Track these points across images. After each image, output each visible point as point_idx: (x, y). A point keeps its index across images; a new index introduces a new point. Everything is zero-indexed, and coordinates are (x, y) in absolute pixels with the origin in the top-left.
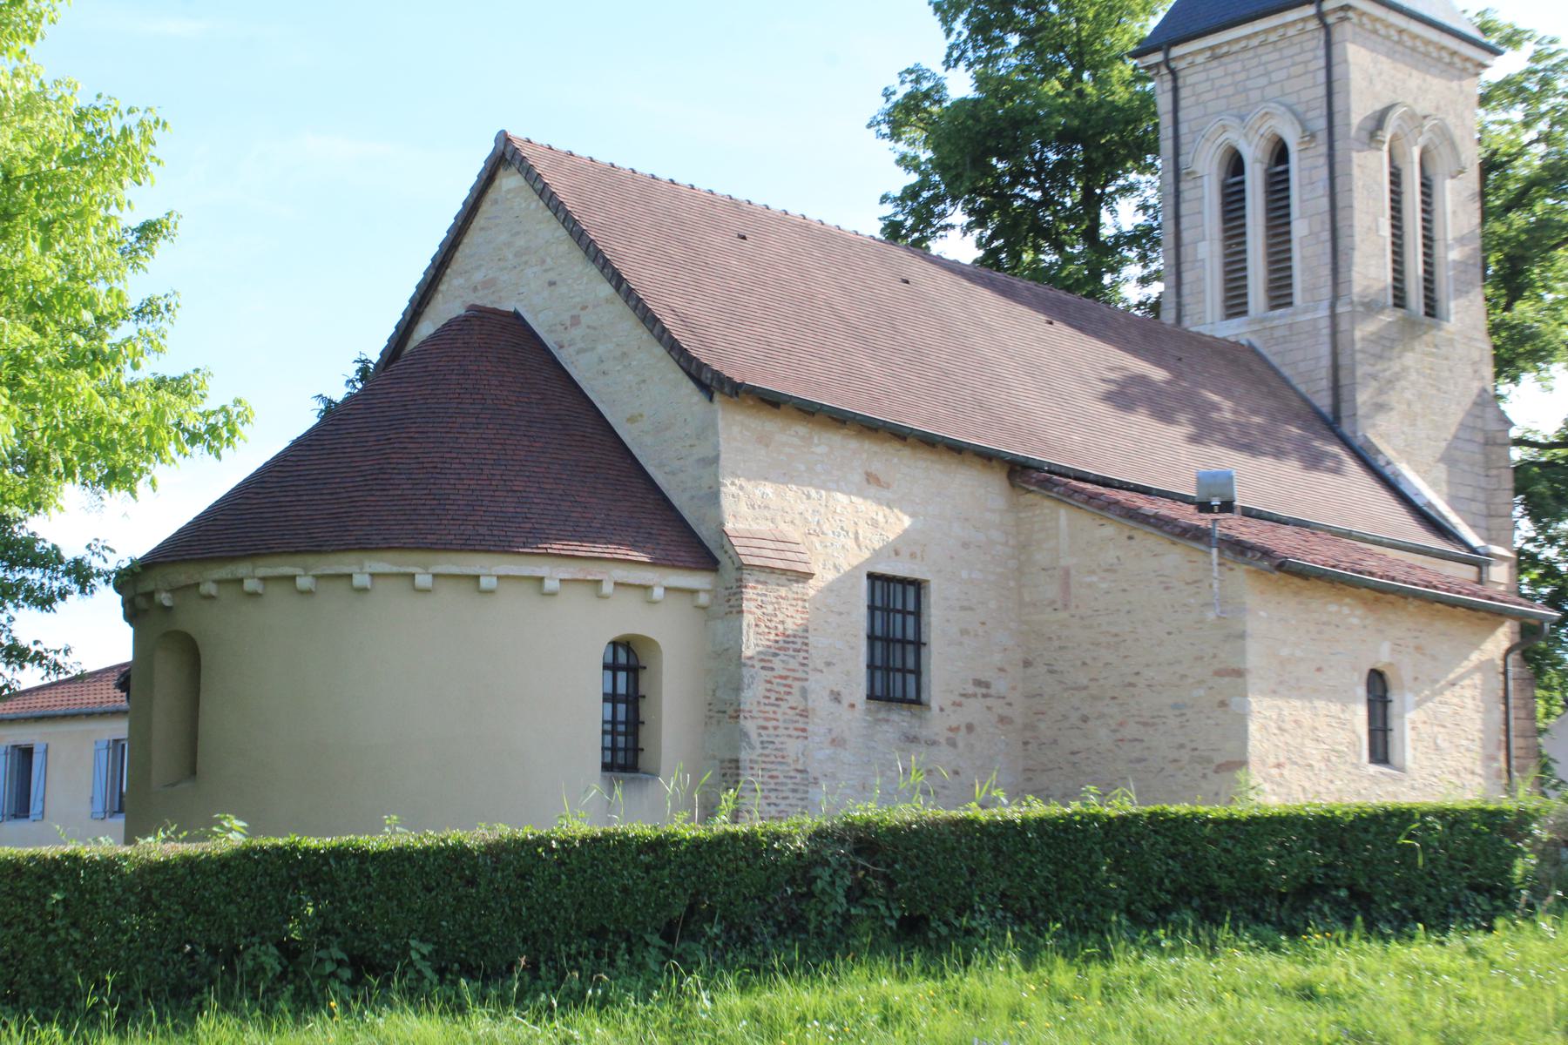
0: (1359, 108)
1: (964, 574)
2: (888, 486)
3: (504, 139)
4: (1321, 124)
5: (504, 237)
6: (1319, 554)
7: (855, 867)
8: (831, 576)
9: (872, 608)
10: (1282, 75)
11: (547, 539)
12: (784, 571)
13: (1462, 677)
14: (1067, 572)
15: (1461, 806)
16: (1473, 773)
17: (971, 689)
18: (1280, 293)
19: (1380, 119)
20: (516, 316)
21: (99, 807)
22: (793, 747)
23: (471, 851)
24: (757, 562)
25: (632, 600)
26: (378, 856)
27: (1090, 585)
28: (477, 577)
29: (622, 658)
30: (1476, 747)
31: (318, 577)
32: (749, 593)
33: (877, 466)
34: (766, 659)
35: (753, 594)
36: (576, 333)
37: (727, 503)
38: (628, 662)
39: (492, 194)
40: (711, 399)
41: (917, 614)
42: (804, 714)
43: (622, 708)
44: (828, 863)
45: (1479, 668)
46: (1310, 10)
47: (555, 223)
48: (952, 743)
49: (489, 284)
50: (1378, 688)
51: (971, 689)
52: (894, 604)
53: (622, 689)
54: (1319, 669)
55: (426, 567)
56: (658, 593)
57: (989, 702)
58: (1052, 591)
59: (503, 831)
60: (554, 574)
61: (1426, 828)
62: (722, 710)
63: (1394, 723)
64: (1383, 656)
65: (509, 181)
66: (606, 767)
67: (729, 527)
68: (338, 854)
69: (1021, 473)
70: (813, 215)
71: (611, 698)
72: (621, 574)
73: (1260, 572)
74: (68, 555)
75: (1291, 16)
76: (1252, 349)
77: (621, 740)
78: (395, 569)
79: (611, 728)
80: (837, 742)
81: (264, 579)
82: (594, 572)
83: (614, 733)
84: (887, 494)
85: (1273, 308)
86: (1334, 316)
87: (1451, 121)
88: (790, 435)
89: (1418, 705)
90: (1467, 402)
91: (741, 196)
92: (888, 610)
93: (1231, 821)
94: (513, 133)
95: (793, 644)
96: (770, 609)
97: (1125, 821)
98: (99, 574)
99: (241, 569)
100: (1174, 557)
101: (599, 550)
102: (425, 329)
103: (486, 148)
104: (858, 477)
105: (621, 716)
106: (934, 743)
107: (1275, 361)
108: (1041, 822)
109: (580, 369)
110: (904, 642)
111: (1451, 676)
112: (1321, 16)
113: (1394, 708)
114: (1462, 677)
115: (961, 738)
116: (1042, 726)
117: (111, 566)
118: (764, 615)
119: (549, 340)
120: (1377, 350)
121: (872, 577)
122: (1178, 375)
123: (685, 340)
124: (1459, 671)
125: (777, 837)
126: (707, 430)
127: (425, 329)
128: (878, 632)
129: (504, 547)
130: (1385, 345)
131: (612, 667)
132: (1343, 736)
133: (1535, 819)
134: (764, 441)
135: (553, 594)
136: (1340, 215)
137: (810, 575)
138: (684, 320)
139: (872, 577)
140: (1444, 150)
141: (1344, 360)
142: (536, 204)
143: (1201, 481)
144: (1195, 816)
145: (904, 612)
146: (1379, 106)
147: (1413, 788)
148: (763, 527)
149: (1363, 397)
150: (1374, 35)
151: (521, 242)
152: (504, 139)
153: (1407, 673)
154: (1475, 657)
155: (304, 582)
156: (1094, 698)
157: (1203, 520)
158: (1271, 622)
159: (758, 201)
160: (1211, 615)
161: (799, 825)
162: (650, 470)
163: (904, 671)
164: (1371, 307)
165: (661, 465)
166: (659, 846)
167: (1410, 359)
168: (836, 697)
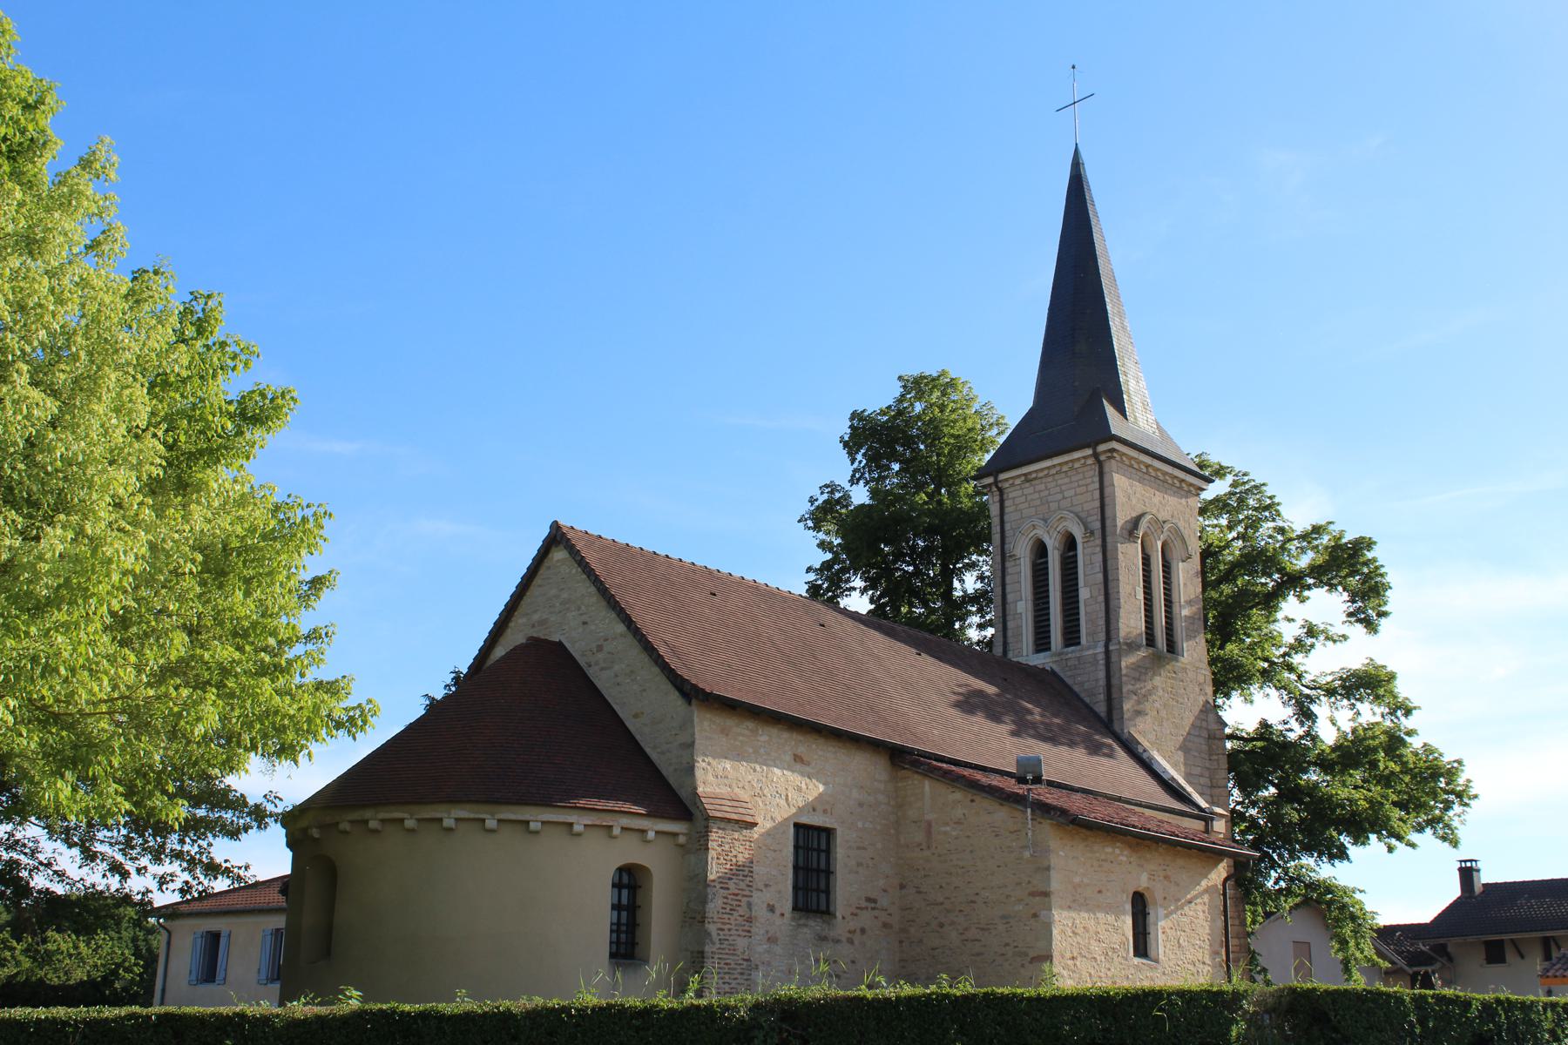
0: (1122, 516)
1: (860, 825)
2: (808, 764)
3: (555, 527)
4: (1098, 525)
5: (554, 592)
6: (1099, 813)
7: (781, 1029)
8: (769, 825)
9: (796, 847)
10: (1072, 492)
11: (576, 797)
12: (737, 822)
13: (1196, 897)
14: (929, 824)
15: (1194, 988)
17: (864, 904)
18: (1072, 635)
19: (1136, 522)
20: (560, 643)
21: (263, 976)
22: (741, 943)
23: (515, 1015)
24: (719, 814)
25: (633, 839)
26: (453, 1018)
27: (945, 833)
28: (527, 823)
29: (625, 879)
31: (419, 820)
32: (713, 836)
33: (801, 750)
34: (724, 881)
35: (715, 836)
36: (600, 655)
37: (699, 774)
38: (630, 881)
39: (546, 563)
40: (690, 703)
41: (828, 851)
42: (749, 920)
43: (624, 914)
44: (762, 1027)
46: (1089, 452)
47: (588, 583)
48: (850, 941)
49: (542, 622)
50: (1140, 907)
51: (864, 904)
52: (812, 844)
53: (624, 901)
55: (493, 814)
56: (651, 835)
57: (876, 913)
58: (919, 837)
59: (539, 1001)
60: (580, 821)
61: (1170, 1003)
62: (693, 915)
63: (1151, 929)
64: (1143, 882)
65: (559, 555)
66: (612, 955)
67: (700, 790)
68: (423, 1016)
69: (900, 757)
70: (761, 580)
71: (616, 907)
72: (626, 821)
73: (1059, 825)
74: (251, 802)
75: (1076, 455)
76: (1053, 672)
77: (623, 936)
78: (472, 816)
79: (616, 928)
80: (772, 940)
81: (383, 821)
82: (607, 820)
83: (618, 931)
84: (808, 769)
85: (1067, 646)
86: (1107, 652)
87: (1181, 524)
88: (743, 729)
89: (1167, 916)
90: (1196, 710)
91: (713, 567)
92: (808, 849)
93: (1039, 999)
94: (562, 522)
95: (742, 872)
96: (727, 847)
97: (968, 999)
98: (271, 815)
99: (368, 814)
100: (1001, 815)
101: (610, 805)
102: (499, 652)
103: (546, 532)
104: (788, 758)
105: (624, 920)
106: (838, 941)
107: (1069, 681)
108: (910, 999)
109: (602, 680)
110: (818, 871)
112: (1096, 455)
113: (1151, 918)
114: (1196, 897)
115: (857, 938)
116: (912, 930)
117: (279, 810)
118: (724, 853)
119: (582, 662)
121: (796, 825)
122: (1004, 690)
123: (674, 663)
124: (1193, 893)
125: (727, 1008)
126: (687, 724)
127: (499, 652)
128: (801, 863)
129: (546, 802)
130: (1141, 672)
131: (617, 885)
132: (1116, 938)
133: (1244, 997)
134: (725, 732)
135: (579, 835)
136: (1111, 585)
137: (756, 824)
138: (673, 649)
139: (796, 825)
140: (1178, 543)
141: (1114, 681)
142: (575, 570)
143: (1019, 762)
144: (1014, 995)
145: (819, 851)
148: (723, 791)
149: (1128, 706)
150: (1134, 470)
151: (565, 595)
152: (555, 527)
154: (1204, 883)
155: (410, 823)
156: (948, 911)
157: (1020, 789)
158: (1068, 861)
159: (725, 570)
160: (1027, 854)
161: (743, 1000)
162: (648, 750)
163: (818, 891)
164: (1132, 646)
165: (655, 748)
166: (647, 1013)
167: (1157, 681)
168: (771, 909)
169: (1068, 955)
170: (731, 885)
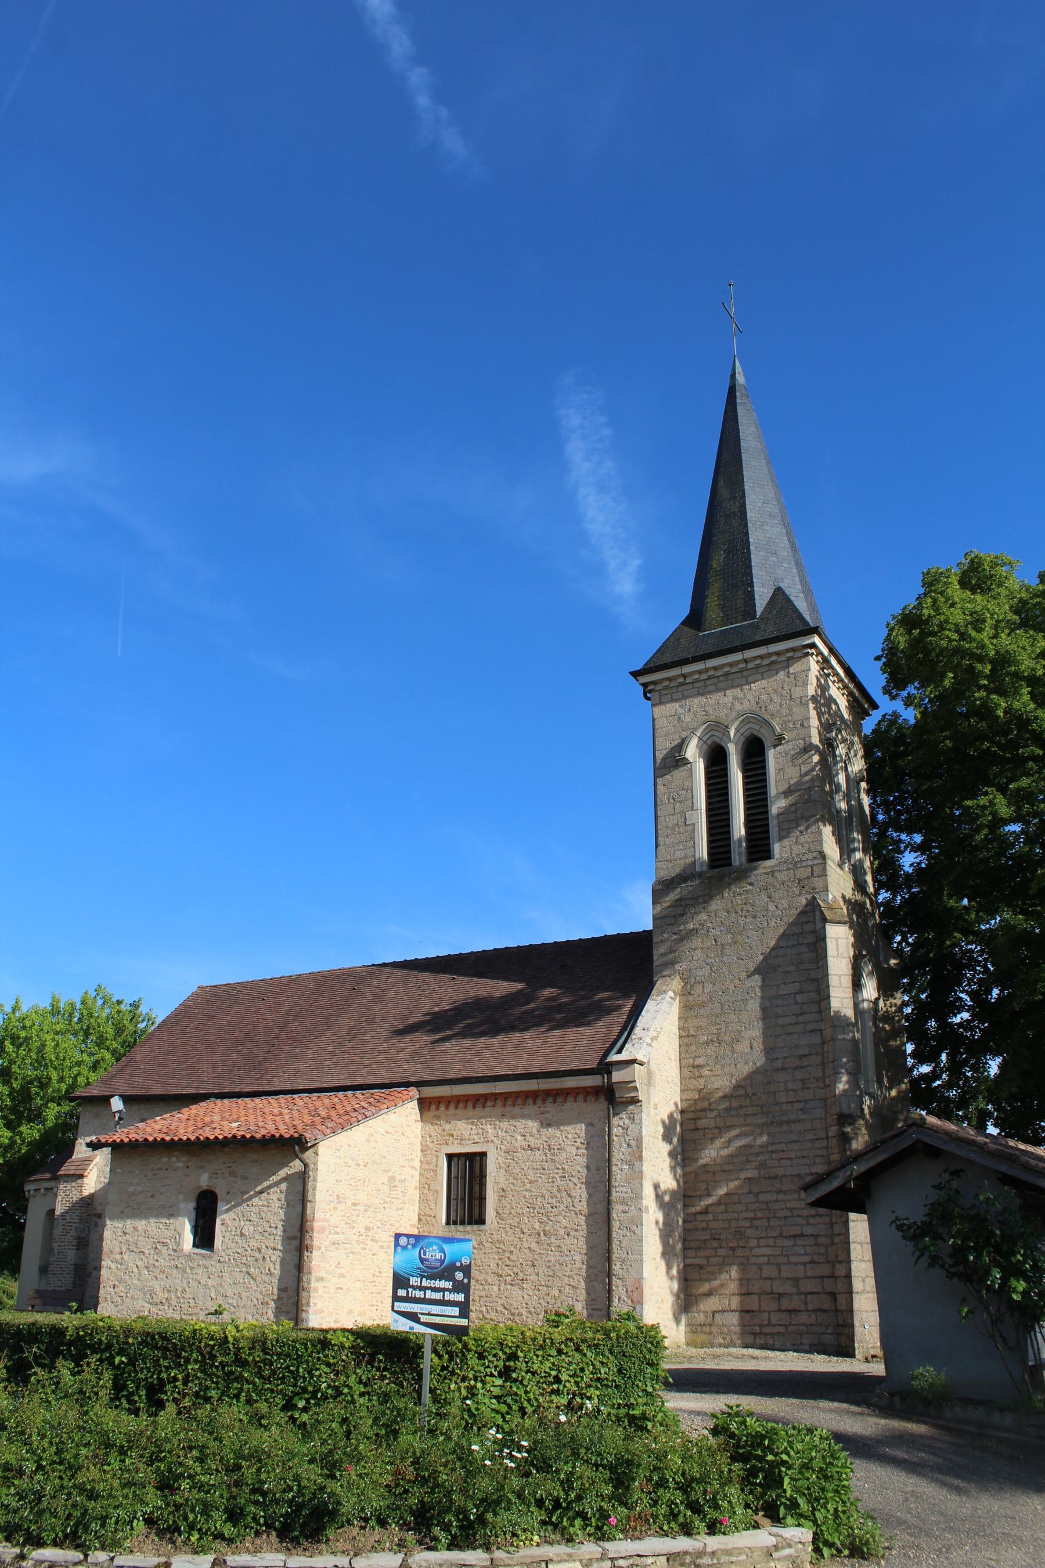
12: (73, 1175)
16: (274, 1249)
19: (681, 746)
30: (280, 1232)
34: (62, 1215)
45: (285, 1179)
54: (152, 1196)
64: (204, 1181)
111: (259, 1188)
120: (680, 910)
124: (266, 1184)
134: (97, 1116)
146: (684, 734)
147: (219, 1261)
153: (220, 1193)
154: (283, 1173)
167: (716, 904)
169: (117, 1250)
170: (68, 1217)
